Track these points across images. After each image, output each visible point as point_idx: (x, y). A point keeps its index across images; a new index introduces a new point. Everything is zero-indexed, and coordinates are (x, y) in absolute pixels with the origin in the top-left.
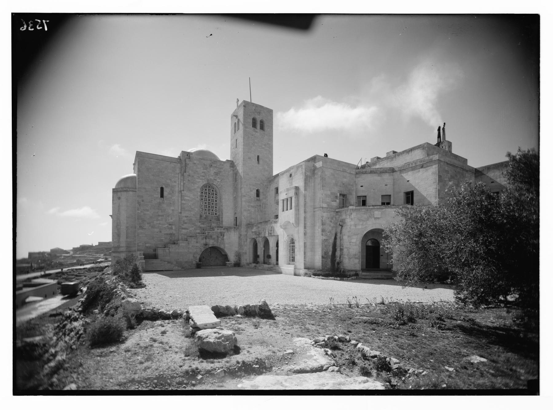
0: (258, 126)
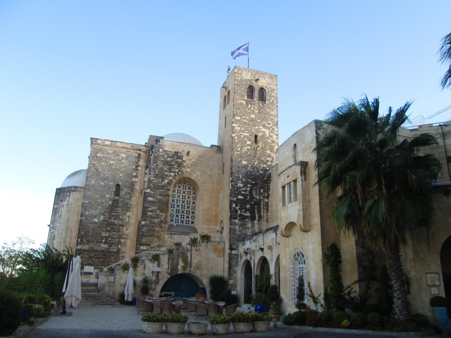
0: (256, 94)
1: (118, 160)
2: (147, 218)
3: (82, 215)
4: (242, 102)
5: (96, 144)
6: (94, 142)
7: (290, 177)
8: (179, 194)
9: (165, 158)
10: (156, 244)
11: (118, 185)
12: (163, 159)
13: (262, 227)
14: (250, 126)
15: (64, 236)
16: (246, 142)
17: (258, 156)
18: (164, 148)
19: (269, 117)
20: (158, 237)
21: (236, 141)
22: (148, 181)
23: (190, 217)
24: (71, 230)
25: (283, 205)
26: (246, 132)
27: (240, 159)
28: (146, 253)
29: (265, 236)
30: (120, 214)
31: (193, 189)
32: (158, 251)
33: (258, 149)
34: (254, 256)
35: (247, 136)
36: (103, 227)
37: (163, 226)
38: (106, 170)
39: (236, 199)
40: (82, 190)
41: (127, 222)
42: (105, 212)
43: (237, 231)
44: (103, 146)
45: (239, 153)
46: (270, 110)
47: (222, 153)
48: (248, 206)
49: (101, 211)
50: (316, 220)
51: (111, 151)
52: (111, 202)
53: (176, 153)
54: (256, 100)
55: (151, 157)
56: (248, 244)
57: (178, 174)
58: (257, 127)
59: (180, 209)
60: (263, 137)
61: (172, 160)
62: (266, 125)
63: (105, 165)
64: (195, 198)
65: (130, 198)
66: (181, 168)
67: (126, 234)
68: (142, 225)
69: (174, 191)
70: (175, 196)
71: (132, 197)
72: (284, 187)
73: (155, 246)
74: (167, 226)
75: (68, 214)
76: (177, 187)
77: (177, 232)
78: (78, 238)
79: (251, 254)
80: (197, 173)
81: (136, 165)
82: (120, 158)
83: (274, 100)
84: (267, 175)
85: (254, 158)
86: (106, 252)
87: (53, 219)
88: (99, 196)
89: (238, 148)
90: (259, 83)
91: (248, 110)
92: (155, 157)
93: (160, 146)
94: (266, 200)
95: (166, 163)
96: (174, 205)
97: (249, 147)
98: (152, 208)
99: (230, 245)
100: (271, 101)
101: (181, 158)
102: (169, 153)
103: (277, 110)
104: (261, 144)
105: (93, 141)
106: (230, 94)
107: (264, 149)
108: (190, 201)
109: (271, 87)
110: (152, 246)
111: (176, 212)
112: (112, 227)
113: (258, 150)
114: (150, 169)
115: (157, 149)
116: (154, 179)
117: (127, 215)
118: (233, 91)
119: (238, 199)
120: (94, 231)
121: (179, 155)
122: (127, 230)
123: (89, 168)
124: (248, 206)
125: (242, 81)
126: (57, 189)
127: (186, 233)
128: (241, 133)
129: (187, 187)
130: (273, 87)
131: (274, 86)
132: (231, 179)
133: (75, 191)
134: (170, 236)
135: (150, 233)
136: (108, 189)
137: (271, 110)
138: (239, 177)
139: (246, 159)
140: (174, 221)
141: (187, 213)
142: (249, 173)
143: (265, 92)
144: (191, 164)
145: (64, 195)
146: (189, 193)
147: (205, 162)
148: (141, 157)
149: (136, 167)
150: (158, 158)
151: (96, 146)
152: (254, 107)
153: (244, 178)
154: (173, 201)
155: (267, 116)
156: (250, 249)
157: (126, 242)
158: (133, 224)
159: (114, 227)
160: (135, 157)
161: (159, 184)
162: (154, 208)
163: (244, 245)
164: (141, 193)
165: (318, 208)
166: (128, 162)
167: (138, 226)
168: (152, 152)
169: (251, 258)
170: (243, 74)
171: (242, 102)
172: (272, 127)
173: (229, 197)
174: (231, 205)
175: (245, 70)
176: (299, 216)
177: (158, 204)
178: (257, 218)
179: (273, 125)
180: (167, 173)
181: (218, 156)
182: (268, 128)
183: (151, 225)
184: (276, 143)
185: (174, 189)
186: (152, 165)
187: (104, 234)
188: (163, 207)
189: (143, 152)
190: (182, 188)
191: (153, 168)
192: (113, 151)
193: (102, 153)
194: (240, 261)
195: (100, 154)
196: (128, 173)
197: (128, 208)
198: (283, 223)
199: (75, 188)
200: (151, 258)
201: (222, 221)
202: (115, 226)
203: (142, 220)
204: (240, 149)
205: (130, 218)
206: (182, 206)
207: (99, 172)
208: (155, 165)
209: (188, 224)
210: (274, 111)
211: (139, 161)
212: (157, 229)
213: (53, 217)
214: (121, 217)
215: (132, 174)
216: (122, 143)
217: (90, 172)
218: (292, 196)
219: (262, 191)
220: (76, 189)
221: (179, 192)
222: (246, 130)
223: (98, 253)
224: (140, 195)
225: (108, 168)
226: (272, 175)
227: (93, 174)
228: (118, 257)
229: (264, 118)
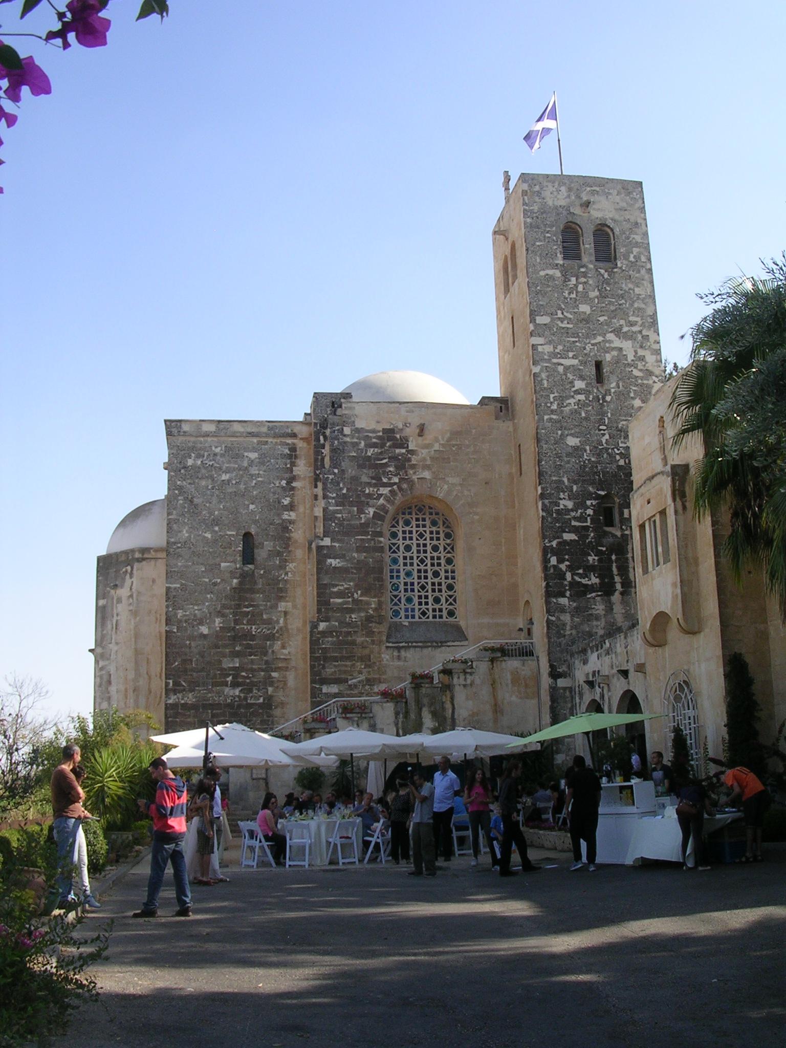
0: (588, 245)
1: (240, 470)
3: (168, 621)
4: (550, 272)
5: (179, 435)
6: (173, 430)
7: (652, 501)
9: (362, 450)
10: (362, 677)
11: (247, 536)
12: (355, 454)
13: (633, 612)
14: (578, 337)
15: (131, 675)
16: (572, 382)
17: (609, 418)
18: (354, 422)
19: (632, 305)
20: (366, 659)
22: (324, 515)
23: (443, 600)
24: (148, 659)
25: (643, 571)
26: (571, 354)
27: (560, 432)
28: (337, 701)
29: (629, 640)
30: (262, 608)
31: (444, 523)
32: (367, 695)
33: (608, 398)
34: (609, 690)
35: (573, 366)
36: (225, 646)
38: (215, 500)
39: (559, 544)
40: (164, 555)
41: (281, 628)
42: (224, 607)
43: (568, 628)
44: (197, 437)
45: (554, 417)
46: (630, 286)
47: (513, 418)
48: (592, 559)
50: (711, 606)
51: (219, 448)
52: (235, 581)
53: (389, 433)
54: (591, 262)
55: (323, 451)
56: (595, 662)
57: (400, 489)
58: (600, 339)
59: (416, 581)
60: (617, 362)
61: (381, 453)
62: (625, 329)
63: (210, 487)
65: (282, 567)
66: (406, 472)
67: (282, 657)
68: (319, 633)
69: (394, 535)
70: (398, 548)
71: (286, 561)
72: (642, 527)
73: (359, 682)
74: (384, 628)
75: (135, 618)
76: (401, 523)
77: (412, 643)
78: (166, 678)
79: (601, 685)
80: (451, 480)
81: (287, 475)
82: (245, 464)
83: (640, 253)
85: (597, 425)
86: (239, 706)
87: (100, 634)
88: (203, 569)
89: (551, 403)
90: (592, 212)
91: (569, 294)
92: (333, 450)
93: (345, 419)
95: (364, 462)
96: (398, 571)
97: (582, 397)
99: (552, 666)
100: (632, 259)
101: (403, 443)
102: (370, 435)
103: (652, 282)
104: (613, 385)
105: (173, 427)
106: (518, 254)
107: (623, 396)
108: (439, 558)
110: (350, 682)
111: (406, 590)
113: (606, 402)
115: (337, 428)
116: (338, 508)
117: (280, 609)
120: (203, 657)
121: (398, 436)
122: (283, 647)
123: (170, 499)
124: (592, 559)
125: (545, 212)
126: (100, 559)
128: (555, 361)
129: (427, 519)
130: (634, 216)
131: (637, 213)
132: (540, 491)
133: (144, 559)
134: (396, 654)
136: (225, 548)
139: (577, 430)
140: (402, 614)
141: (433, 591)
143: (613, 234)
144: (432, 458)
145: (117, 572)
146: (434, 535)
148: (298, 453)
149: (289, 482)
150: (343, 451)
151: (181, 439)
152: (585, 283)
153: (576, 484)
154: (395, 561)
155: (623, 301)
156: (599, 671)
157: (285, 677)
158: (298, 630)
160: (283, 456)
161: (353, 522)
162: (345, 586)
163: (585, 662)
164: (310, 548)
165: (713, 578)
166: (265, 471)
167: (311, 636)
169: (602, 696)
170: (547, 194)
171: (550, 272)
174: (545, 561)
175: (549, 181)
176: (675, 597)
177: (355, 574)
178: (618, 586)
179: (645, 326)
180: (371, 489)
181: (505, 426)
185: (394, 529)
186: (329, 472)
187: (227, 663)
188: (371, 580)
189: (301, 439)
190: (414, 526)
191: (332, 479)
192: (226, 447)
194: (580, 703)
196: (268, 501)
197: (281, 590)
198: (646, 613)
199: (143, 555)
201: (527, 602)
204: (558, 404)
206: (419, 571)
207: (196, 506)
208: (336, 471)
209: (441, 617)
210: (643, 285)
211: (293, 464)
212: (360, 640)
213: (99, 629)
214: (265, 617)
215: (279, 502)
216: (243, 424)
218: (660, 550)
221: (407, 535)
223: (219, 711)
224: (307, 558)
225: (217, 492)
227: (183, 515)
228: (268, 717)
229: (616, 310)
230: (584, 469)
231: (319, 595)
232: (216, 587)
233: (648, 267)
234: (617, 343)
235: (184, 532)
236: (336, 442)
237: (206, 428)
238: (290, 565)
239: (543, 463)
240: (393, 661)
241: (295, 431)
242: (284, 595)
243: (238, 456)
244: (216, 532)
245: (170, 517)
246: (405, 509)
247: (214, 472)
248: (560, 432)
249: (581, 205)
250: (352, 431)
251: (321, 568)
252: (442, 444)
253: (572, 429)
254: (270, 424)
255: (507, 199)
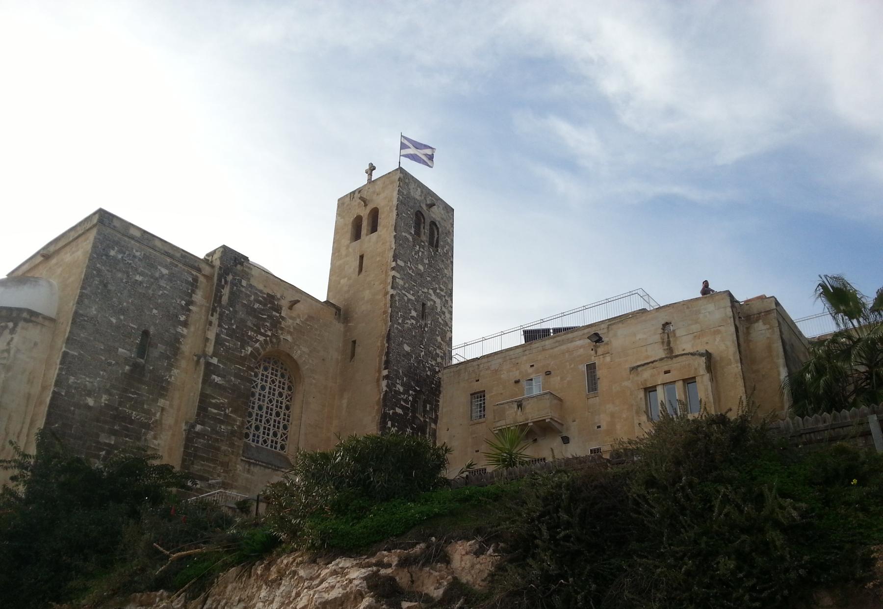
0: (425, 231)
2: (206, 420)
3: (58, 383)
4: (408, 236)
8: (264, 383)
10: (219, 480)
14: (416, 283)
16: (410, 310)
18: (250, 279)
19: (442, 278)
20: (225, 465)
21: (397, 305)
23: (279, 436)
26: (411, 292)
28: (221, 492)
30: (144, 398)
31: (289, 378)
33: (426, 329)
35: (412, 300)
37: (236, 443)
39: (393, 413)
41: (156, 421)
44: (123, 235)
45: (400, 328)
46: (443, 266)
49: (106, 382)
52: (127, 368)
53: (271, 298)
54: (427, 241)
57: (271, 342)
59: (264, 415)
60: (433, 309)
61: (263, 310)
62: (438, 291)
63: (124, 281)
64: (290, 398)
65: (169, 368)
71: (172, 366)
77: (259, 462)
82: (157, 275)
84: (436, 381)
85: (419, 343)
88: (102, 348)
92: (232, 293)
94: (433, 426)
95: (252, 312)
97: (414, 322)
98: (219, 399)
101: (278, 309)
102: (259, 293)
104: (429, 322)
107: (433, 331)
109: (446, 225)
110: (210, 482)
111: (256, 420)
112: (123, 424)
113: (425, 331)
114: (221, 315)
115: (238, 278)
116: (227, 338)
117: (159, 404)
118: (391, 211)
119: (395, 413)
121: (276, 303)
122: (155, 438)
127: (275, 466)
128: (404, 292)
129: (279, 371)
132: (385, 372)
134: (247, 466)
135: (211, 455)
137: (444, 265)
138: (397, 371)
140: (251, 437)
142: (412, 370)
143: (438, 231)
144: (294, 328)
147: (316, 330)
148: (198, 284)
151: (109, 230)
155: (438, 274)
159: (129, 426)
160: (187, 282)
162: (221, 401)
164: (198, 362)
166: (171, 287)
167: (189, 433)
168: (226, 282)
171: (408, 236)
172: (445, 296)
173: (376, 408)
180: (252, 333)
181: (339, 327)
182: (440, 297)
183: (214, 436)
184: (449, 327)
187: (104, 439)
189: (204, 275)
192: (144, 254)
193: (121, 251)
195: (116, 252)
196: (169, 312)
197: (163, 388)
200: (234, 506)
202: (131, 424)
203: (197, 422)
204: (402, 321)
205: (164, 413)
206: (268, 408)
207: (109, 291)
208: (231, 309)
209: (276, 448)
211: (193, 292)
212: (224, 448)
214: (145, 406)
215: (177, 317)
217: (90, 286)
219: (428, 406)
220: (33, 319)
221: (264, 378)
222: (410, 289)
225: (129, 287)
226: (442, 383)
230: (411, 369)
231: (201, 401)
232: (110, 367)
233: (452, 260)
234: (433, 297)
235: (93, 309)
236: (235, 288)
237: (132, 231)
238: (175, 370)
239: (391, 355)
240: (244, 473)
241: (200, 267)
242: (165, 393)
243: (152, 266)
244: (121, 320)
245: (84, 291)
246: (268, 358)
247: (130, 270)
248: (401, 339)
249: (427, 205)
250: (247, 285)
251: (206, 380)
252: (302, 321)
253: (407, 340)
254: (184, 253)
255: (370, 181)
